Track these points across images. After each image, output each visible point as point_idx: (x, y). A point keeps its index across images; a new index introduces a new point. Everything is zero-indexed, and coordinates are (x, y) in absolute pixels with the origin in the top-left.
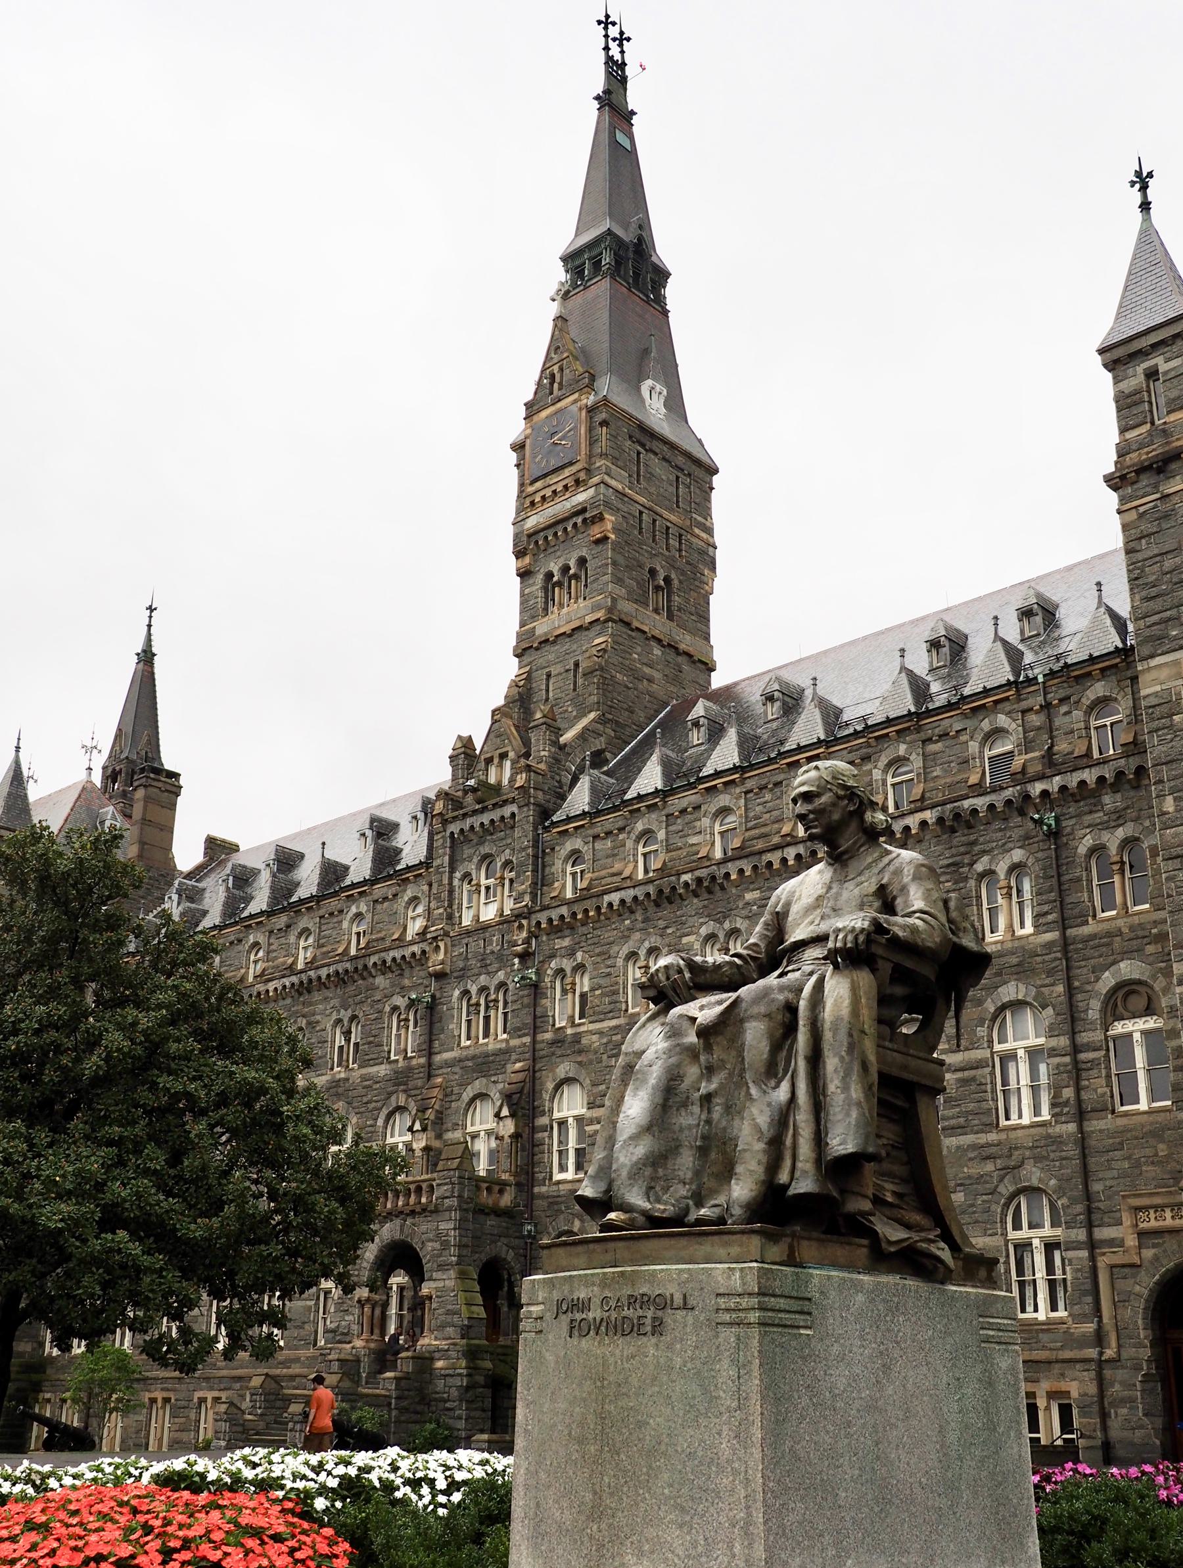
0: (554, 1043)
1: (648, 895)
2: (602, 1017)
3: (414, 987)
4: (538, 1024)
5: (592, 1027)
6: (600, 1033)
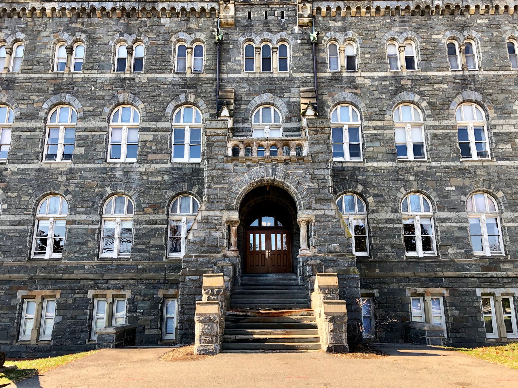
0: (331, 79)
1: (408, 7)
2: (373, 70)
3: (201, 30)
4: (319, 67)
5: (364, 74)
6: (371, 78)
